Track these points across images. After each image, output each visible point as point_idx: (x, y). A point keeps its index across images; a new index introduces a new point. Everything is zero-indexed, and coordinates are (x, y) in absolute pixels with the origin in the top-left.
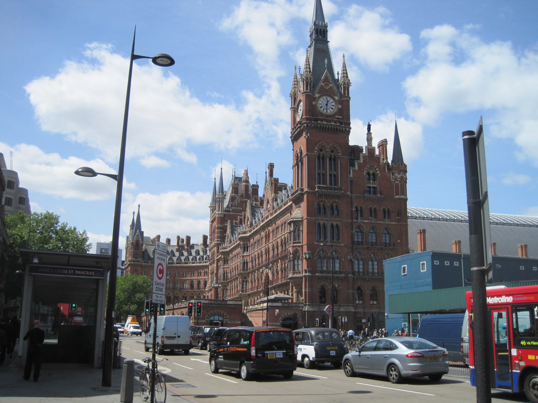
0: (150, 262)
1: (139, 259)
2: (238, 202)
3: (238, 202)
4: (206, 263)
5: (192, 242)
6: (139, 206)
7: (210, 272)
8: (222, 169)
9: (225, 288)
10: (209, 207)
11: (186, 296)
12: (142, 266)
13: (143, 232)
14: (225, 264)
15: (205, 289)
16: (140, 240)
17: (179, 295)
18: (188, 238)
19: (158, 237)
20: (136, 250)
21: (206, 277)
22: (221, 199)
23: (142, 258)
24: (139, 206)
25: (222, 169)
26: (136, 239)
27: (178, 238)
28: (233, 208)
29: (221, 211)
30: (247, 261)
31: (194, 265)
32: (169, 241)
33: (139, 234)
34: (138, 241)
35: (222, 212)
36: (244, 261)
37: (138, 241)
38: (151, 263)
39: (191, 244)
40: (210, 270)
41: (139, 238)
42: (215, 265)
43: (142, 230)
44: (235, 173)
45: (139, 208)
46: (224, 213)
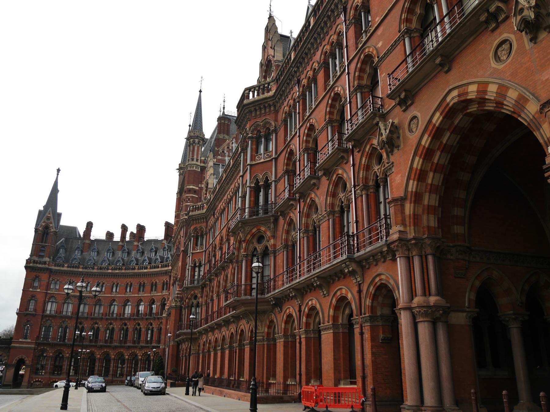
0: (66, 265)
1: (47, 259)
2: (228, 148)
3: (228, 148)
4: (166, 266)
5: (148, 236)
6: (59, 170)
7: (172, 282)
8: (200, 91)
9: (195, 302)
10: (177, 169)
11: (127, 328)
12: (50, 271)
13: (60, 215)
14: (197, 245)
15: (162, 314)
16: (52, 225)
17: (115, 326)
18: (141, 229)
19: (90, 225)
20: (42, 242)
21: (165, 292)
22: (197, 140)
23: (52, 257)
24: (59, 170)
25: (200, 91)
26: (44, 224)
27: (124, 228)
28: (220, 157)
29: (197, 160)
30: (267, 179)
31: (145, 271)
32: (110, 235)
33: (51, 215)
34: (47, 227)
35: (199, 163)
36: (257, 182)
37: (47, 227)
38: (68, 267)
39: (145, 239)
40: (172, 278)
41: (51, 223)
42: (180, 264)
43: (59, 211)
44: (224, 108)
45: (58, 174)
46: (202, 165)
